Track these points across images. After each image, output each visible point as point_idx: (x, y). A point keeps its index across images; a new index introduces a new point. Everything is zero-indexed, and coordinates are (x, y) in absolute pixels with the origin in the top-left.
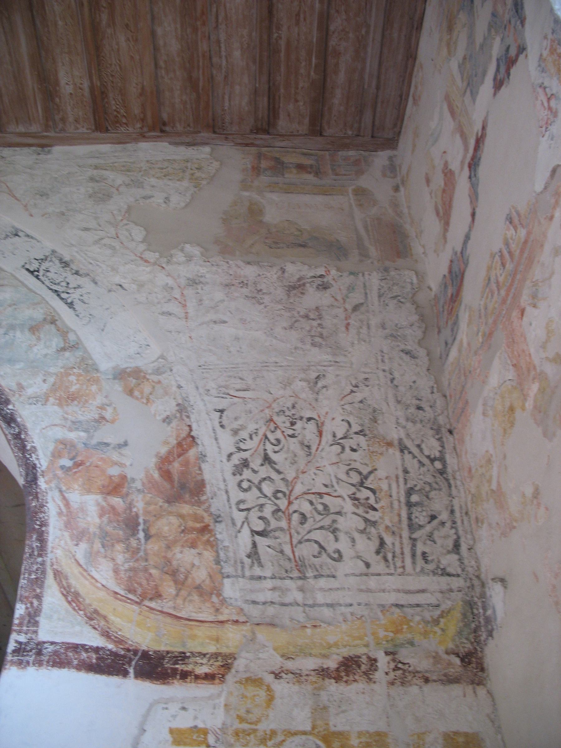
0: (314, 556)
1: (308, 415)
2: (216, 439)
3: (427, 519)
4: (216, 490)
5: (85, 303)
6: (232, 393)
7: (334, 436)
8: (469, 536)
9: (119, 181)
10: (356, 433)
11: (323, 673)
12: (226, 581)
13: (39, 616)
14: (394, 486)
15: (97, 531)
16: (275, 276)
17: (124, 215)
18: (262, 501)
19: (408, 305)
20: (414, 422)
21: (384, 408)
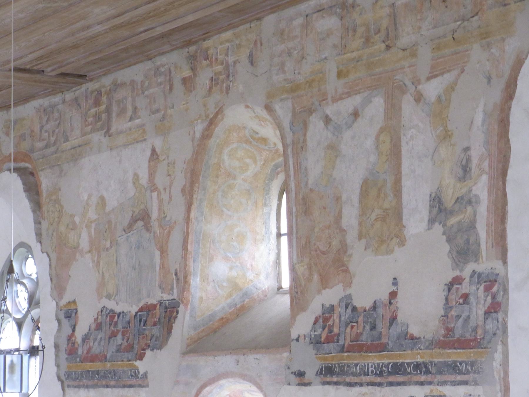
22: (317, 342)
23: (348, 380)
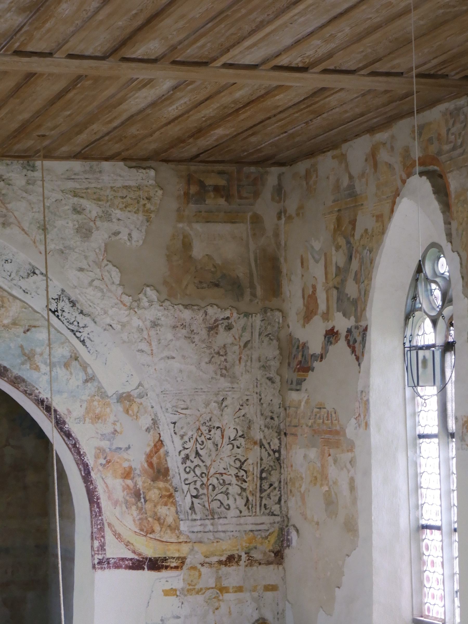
0: (218, 508)
1: (217, 426)
2: (173, 442)
3: (268, 486)
4: (174, 473)
5: (92, 341)
6: (180, 411)
7: (229, 439)
8: (286, 496)
9: (94, 214)
10: (240, 437)
11: (220, 562)
12: (181, 522)
13: (105, 546)
14: (255, 468)
15: (123, 500)
16: (201, 318)
17: (104, 255)
18: (196, 478)
19: (275, 341)
20: (268, 428)
21: (255, 419)
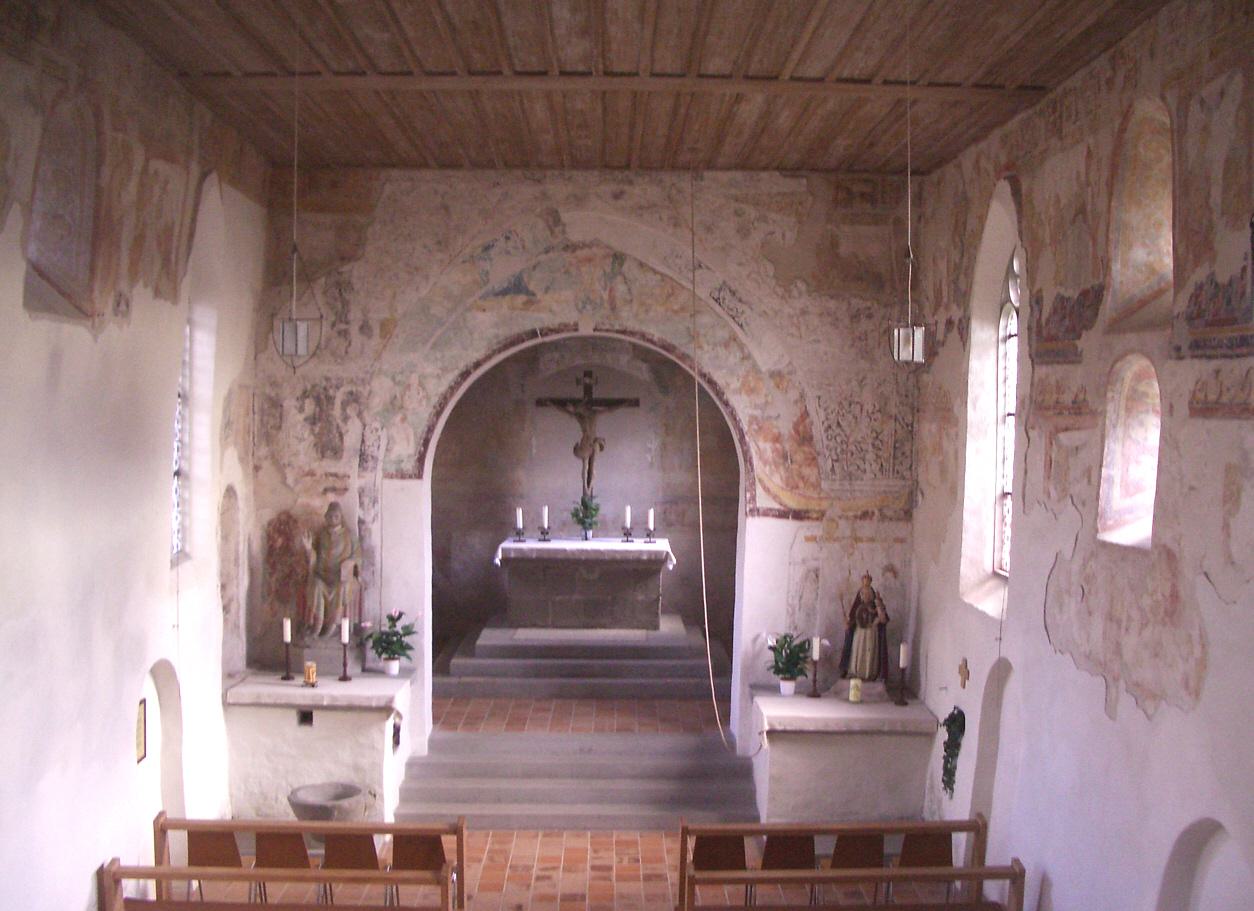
9: (753, 216)
11: (856, 517)
22: (1190, 319)
23: (1208, 353)
